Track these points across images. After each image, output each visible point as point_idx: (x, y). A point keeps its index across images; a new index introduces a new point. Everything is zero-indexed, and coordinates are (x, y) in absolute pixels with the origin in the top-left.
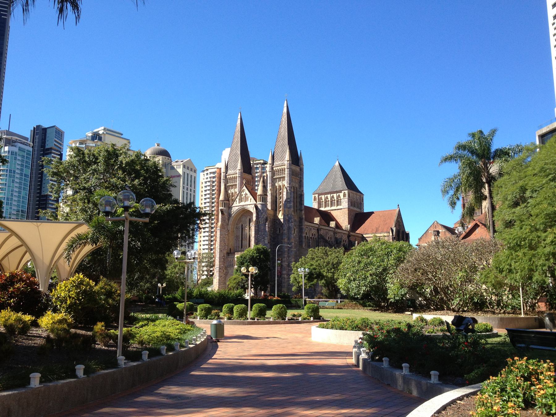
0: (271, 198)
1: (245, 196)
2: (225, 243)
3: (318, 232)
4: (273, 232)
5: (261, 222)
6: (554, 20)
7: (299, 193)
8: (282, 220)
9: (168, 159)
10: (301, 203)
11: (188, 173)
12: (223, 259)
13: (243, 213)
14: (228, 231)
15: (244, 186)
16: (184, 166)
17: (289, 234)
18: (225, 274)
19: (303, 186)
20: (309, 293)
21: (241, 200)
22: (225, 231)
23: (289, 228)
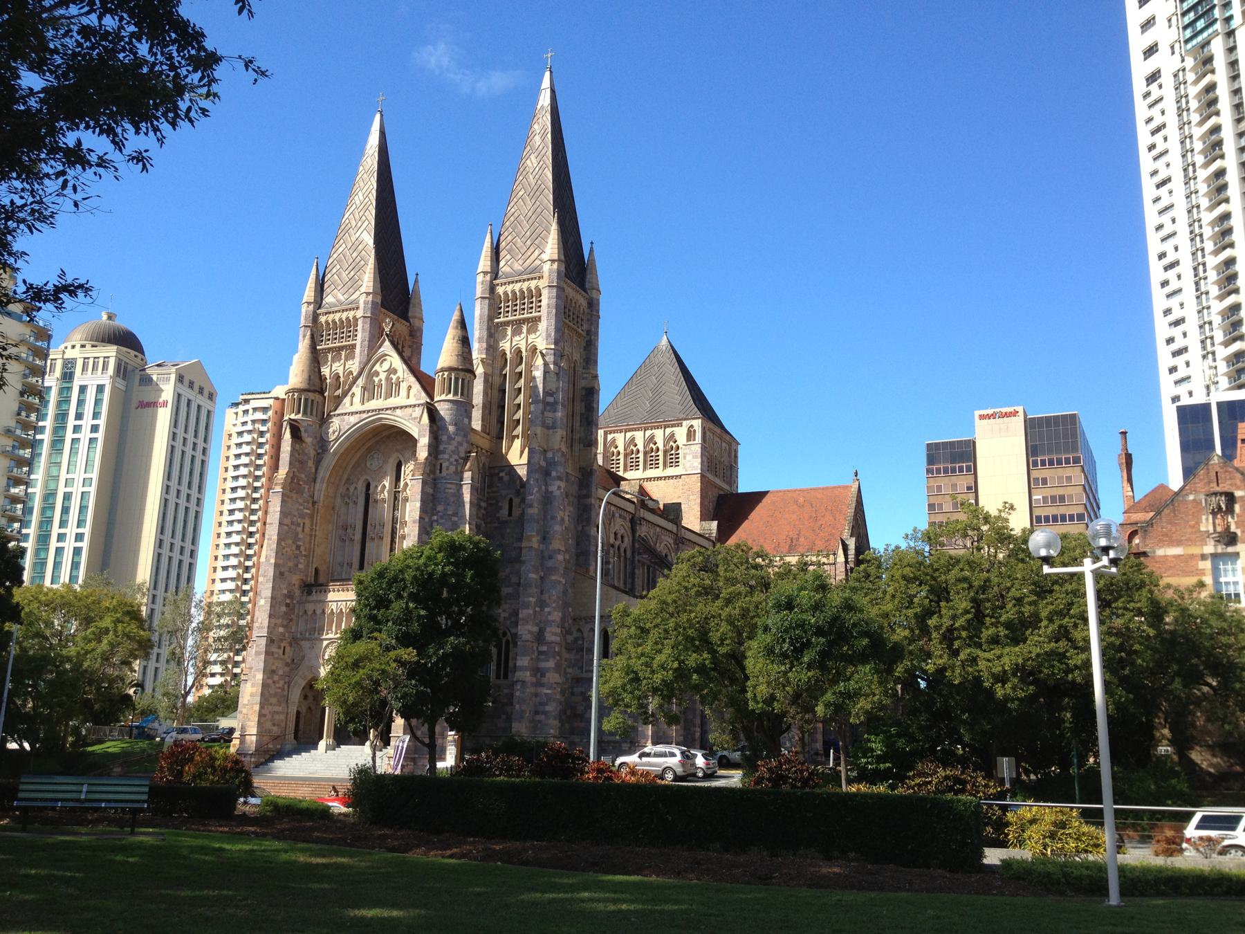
0: (485, 393)
1: (388, 379)
2: (298, 547)
3: (633, 531)
4: (483, 512)
5: (448, 468)
6: (1148, 85)
7: (583, 383)
8: (522, 472)
9: (136, 356)
10: (587, 418)
11: (191, 398)
12: (288, 605)
14: (314, 503)
15: (384, 340)
16: (180, 379)
17: (545, 518)
18: (287, 664)
19: (596, 362)
20: (609, 742)
21: (370, 391)
22: (301, 501)
23: (547, 499)
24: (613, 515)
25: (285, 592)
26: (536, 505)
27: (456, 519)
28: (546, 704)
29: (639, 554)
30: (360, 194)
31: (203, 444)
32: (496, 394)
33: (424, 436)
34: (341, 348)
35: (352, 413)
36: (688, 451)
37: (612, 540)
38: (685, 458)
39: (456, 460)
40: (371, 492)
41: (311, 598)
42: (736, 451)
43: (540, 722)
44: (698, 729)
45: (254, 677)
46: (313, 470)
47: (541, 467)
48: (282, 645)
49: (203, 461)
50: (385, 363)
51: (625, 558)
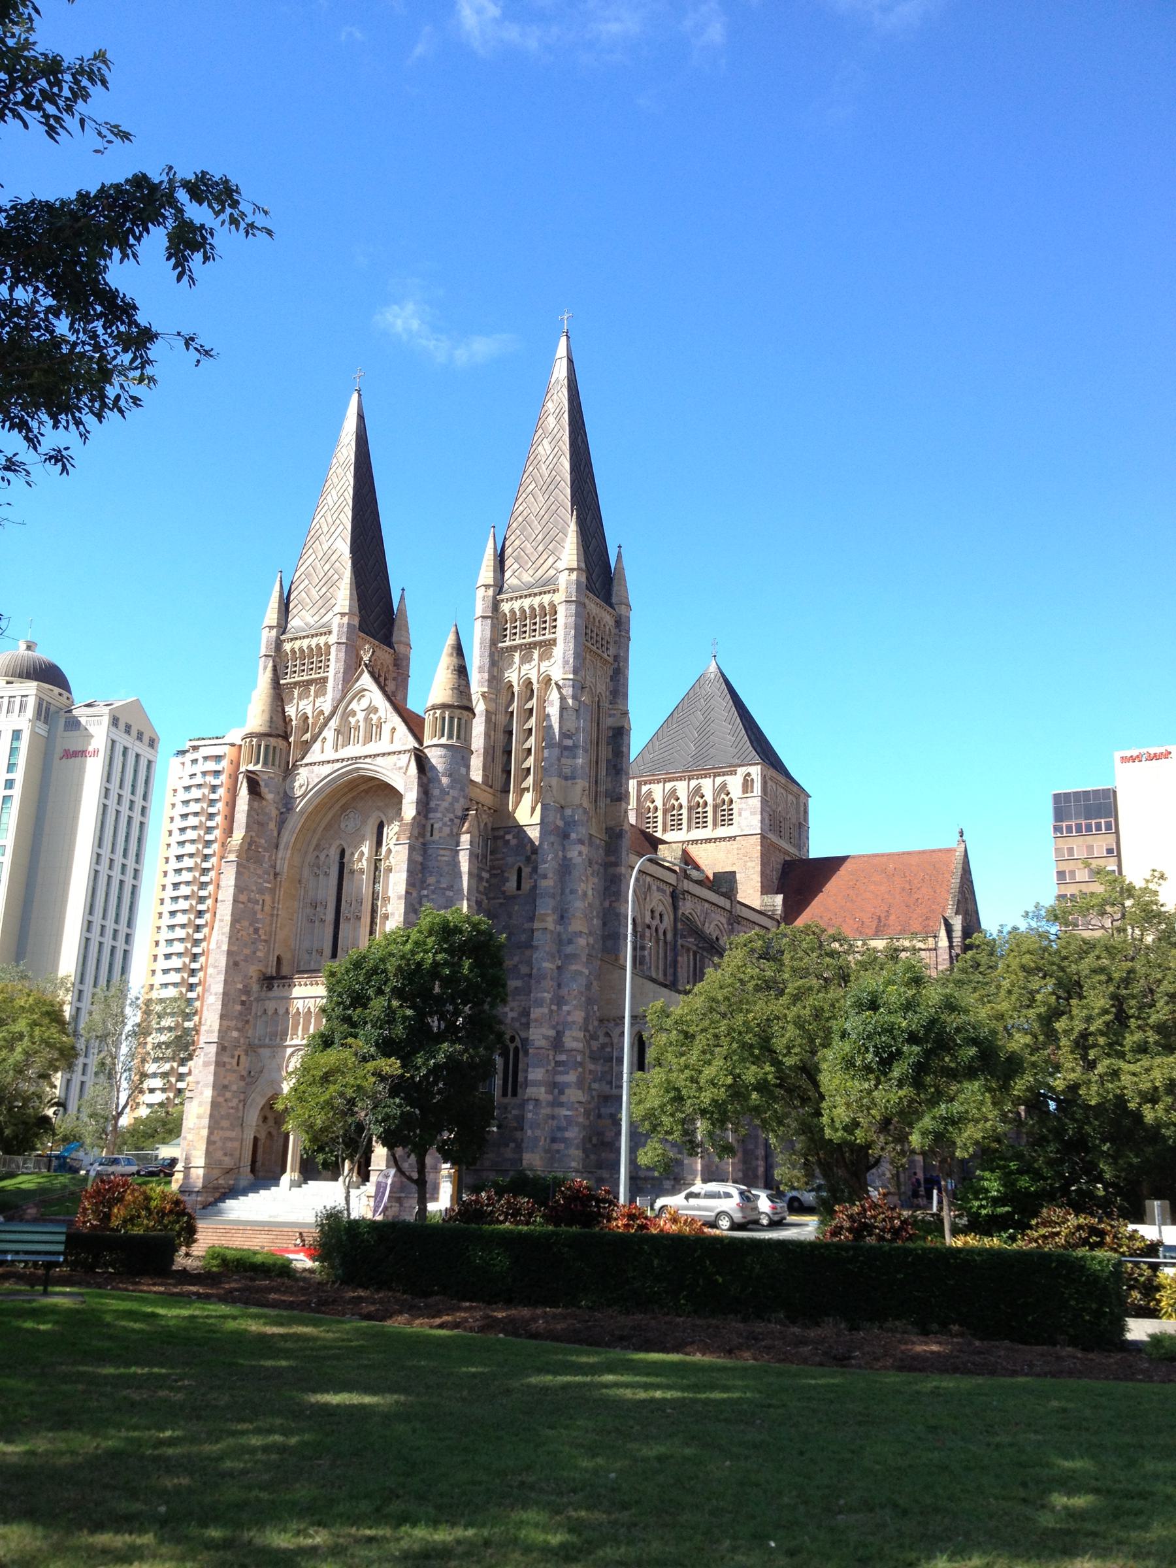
0: (487, 735)
1: (367, 719)
2: (256, 931)
3: (675, 908)
4: (485, 884)
5: (441, 830)
7: (610, 722)
8: (534, 834)
10: (615, 766)
11: (128, 745)
12: (243, 1003)
13: (350, 796)
14: (276, 875)
15: (363, 671)
16: (115, 722)
17: (562, 893)
18: (242, 1078)
19: (626, 695)
20: (646, 1179)
21: (345, 734)
22: (259, 872)
23: (565, 868)
24: (649, 887)
25: (240, 986)
26: (550, 875)
27: (451, 894)
28: (566, 1129)
29: (683, 937)
30: (334, 492)
31: (142, 803)
32: (501, 736)
33: (411, 789)
34: (309, 683)
35: (323, 763)
36: (744, 806)
37: (648, 920)
38: (740, 815)
39: (452, 820)
40: (345, 860)
41: (271, 994)
42: (806, 806)
43: (558, 1151)
44: (761, 1163)
45: (201, 1093)
46: (275, 834)
47: (558, 827)
48: (237, 1053)
49: (142, 823)
50: (363, 700)
51: (665, 942)
